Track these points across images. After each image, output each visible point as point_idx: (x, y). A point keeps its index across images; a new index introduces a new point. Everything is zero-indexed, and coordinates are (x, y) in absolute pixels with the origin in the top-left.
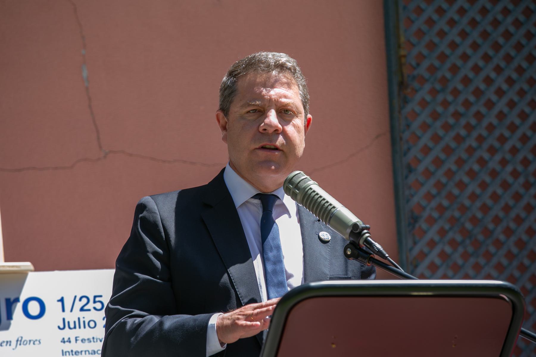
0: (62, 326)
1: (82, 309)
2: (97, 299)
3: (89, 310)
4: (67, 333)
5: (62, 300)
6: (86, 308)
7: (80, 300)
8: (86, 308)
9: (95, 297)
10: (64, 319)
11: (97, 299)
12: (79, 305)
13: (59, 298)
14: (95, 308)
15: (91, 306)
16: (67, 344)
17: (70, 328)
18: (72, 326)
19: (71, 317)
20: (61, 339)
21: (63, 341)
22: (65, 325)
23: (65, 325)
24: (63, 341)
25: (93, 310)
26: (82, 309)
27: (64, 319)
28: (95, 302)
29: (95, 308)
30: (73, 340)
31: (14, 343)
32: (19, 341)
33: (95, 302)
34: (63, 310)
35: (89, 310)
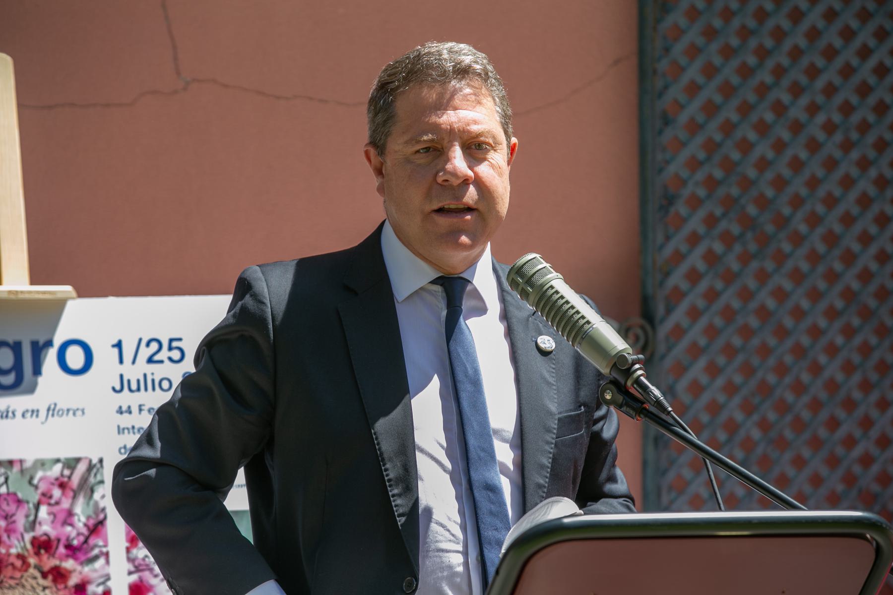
0: (118, 387)
1: (150, 360)
2: (175, 344)
3: (161, 362)
4: (126, 399)
5: (119, 345)
6: (156, 358)
7: (148, 345)
8: (156, 358)
9: (171, 340)
10: (121, 376)
11: (175, 344)
12: (145, 353)
13: (115, 342)
14: (170, 359)
15: (164, 355)
16: (126, 415)
17: (130, 390)
18: (134, 386)
19: (133, 373)
20: (117, 408)
21: (120, 411)
22: (123, 386)
23: (123, 386)
24: (120, 411)
25: (167, 362)
26: (150, 360)
27: (121, 376)
28: (170, 349)
29: (170, 359)
30: (135, 409)
31: (43, 413)
32: (52, 410)
33: (170, 349)
34: (121, 361)
35: (161, 362)
